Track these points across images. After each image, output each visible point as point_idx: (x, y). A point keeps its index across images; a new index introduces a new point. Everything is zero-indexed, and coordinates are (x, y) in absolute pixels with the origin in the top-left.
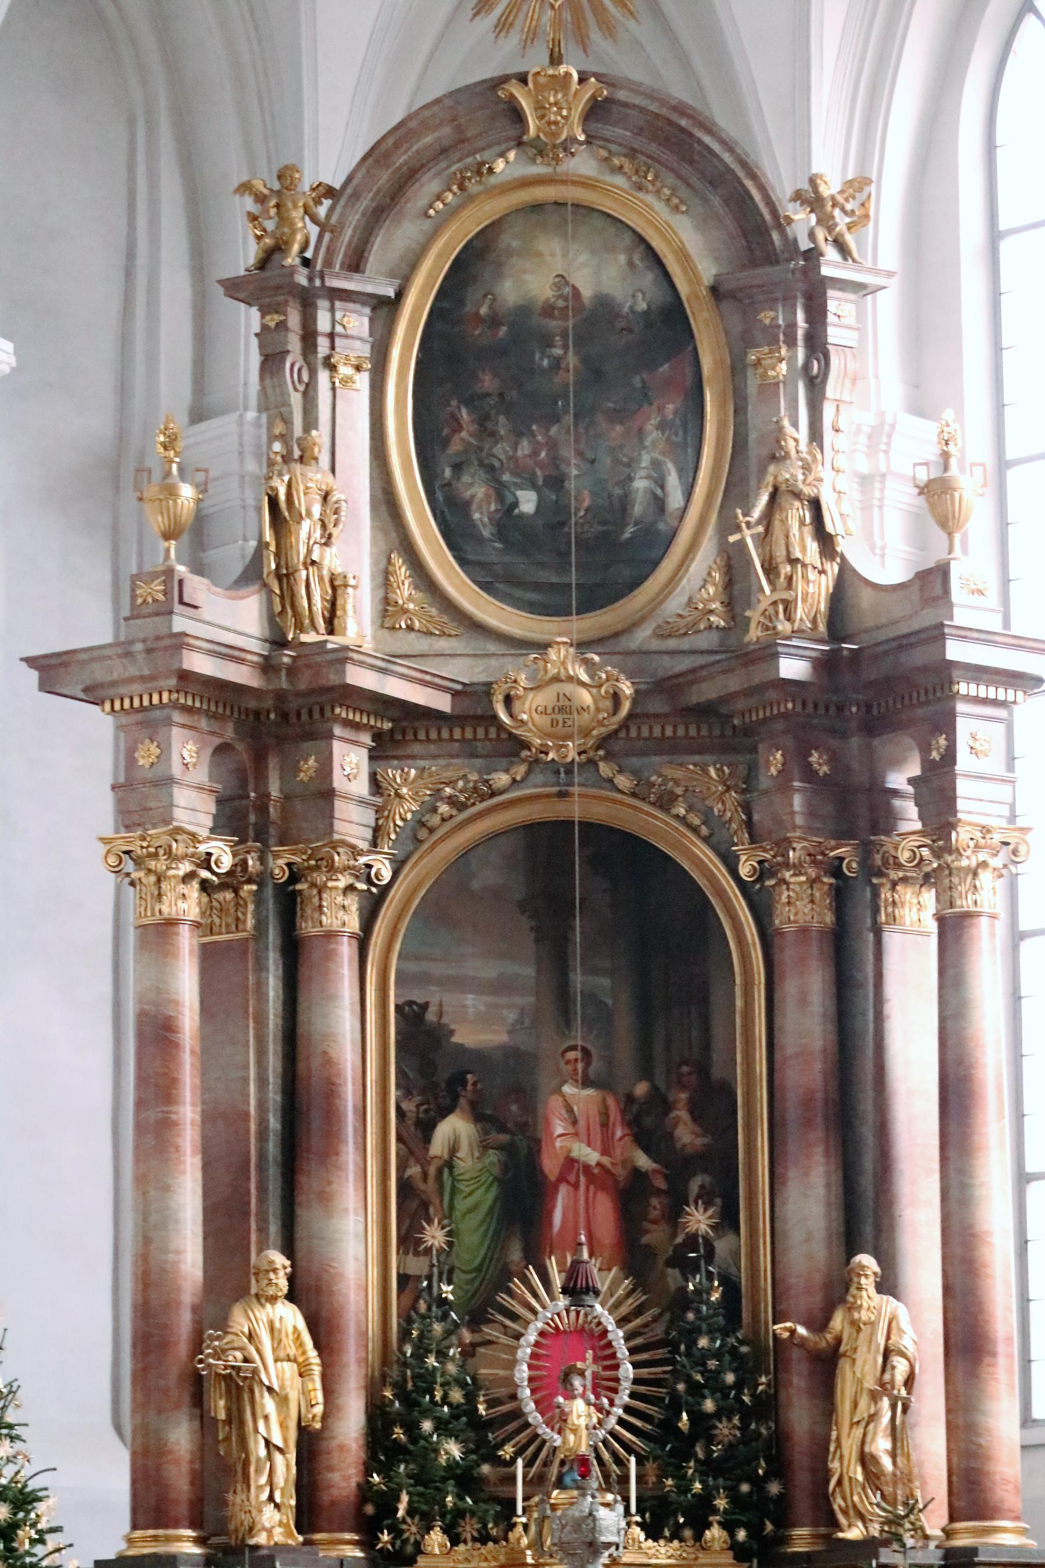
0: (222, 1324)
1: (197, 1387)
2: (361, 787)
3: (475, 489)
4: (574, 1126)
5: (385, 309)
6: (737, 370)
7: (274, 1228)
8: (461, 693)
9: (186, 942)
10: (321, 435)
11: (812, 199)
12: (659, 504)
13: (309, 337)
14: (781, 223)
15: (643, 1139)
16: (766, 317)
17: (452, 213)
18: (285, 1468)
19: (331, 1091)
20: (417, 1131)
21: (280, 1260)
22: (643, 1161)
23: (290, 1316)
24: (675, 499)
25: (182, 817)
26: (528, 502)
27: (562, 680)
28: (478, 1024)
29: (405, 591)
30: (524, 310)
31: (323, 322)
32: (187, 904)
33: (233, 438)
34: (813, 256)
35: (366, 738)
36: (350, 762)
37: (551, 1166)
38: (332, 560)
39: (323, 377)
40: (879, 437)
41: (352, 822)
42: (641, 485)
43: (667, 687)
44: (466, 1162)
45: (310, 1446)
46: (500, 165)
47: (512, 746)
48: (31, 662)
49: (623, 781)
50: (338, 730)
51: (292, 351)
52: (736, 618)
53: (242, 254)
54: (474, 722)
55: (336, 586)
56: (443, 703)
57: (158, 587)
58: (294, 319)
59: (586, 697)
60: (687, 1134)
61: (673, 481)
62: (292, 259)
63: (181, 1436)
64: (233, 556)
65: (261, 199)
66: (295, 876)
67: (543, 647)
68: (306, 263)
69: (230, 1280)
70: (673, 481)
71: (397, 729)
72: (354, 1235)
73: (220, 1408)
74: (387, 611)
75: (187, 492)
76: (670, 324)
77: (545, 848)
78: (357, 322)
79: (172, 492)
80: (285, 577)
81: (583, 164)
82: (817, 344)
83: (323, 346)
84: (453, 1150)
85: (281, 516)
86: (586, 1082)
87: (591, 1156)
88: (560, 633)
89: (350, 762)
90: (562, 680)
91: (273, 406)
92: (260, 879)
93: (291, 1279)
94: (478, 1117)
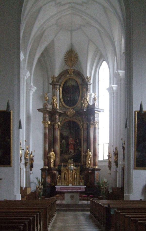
0: (49, 153)
1: (48, 157)
2: (58, 118)
3: (66, 98)
4: (71, 141)
5: (60, 86)
6: (82, 90)
7: (52, 147)
8: (64, 112)
9: (47, 128)
10: (56, 94)
11: (87, 78)
12: (77, 99)
13: (55, 88)
14: (85, 80)
15: (75, 142)
16: (84, 86)
17: (64, 79)
18: (53, 162)
19: (56, 139)
20: (61, 141)
21: (53, 149)
22: (75, 143)
23: (53, 153)
24: (78, 99)
25: (47, 120)
26: (69, 99)
27: (71, 111)
28: (65, 134)
29: (61, 105)
30: (69, 85)
31: (56, 86)
32: (47, 126)
33: (50, 94)
34: (87, 82)
35: (58, 115)
36: (57, 117)
37: (69, 143)
38: (56, 103)
39: (56, 90)
40: (91, 95)
41: (57, 120)
42: (76, 98)
43: (78, 111)
44: (64, 143)
45: (55, 161)
46: (67, 76)
47: (67, 115)
48: (38, 109)
49: (74, 118)
50: (56, 114)
51: (54, 88)
52: (82, 107)
53: (51, 81)
54: (65, 114)
55: (57, 104)
56: (63, 112)
57: (45, 104)
58: (54, 86)
59: (72, 112)
60: (78, 141)
61: (78, 98)
62: (54, 82)
63: (47, 160)
64: (50, 102)
65: (52, 78)
66: (54, 124)
67: (69, 109)
68: (55, 82)
69: (50, 151)
70: (78, 98)
71: (60, 114)
72: (57, 148)
73: (49, 158)
74: (60, 106)
75: (47, 98)
76: (78, 87)
77: (70, 122)
78: (58, 86)
79: (46, 98)
80: (53, 104)
81: (73, 75)
82: (87, 88)
83: (56, 88)
84: (64, 142)
85: (53, 100)
86: (72, 138)
87: (72, 143)
88: (71, 108)
89: (57, 117)
90: (71, 111)
91: (53, 92)
92: (52, 124)
93: (53, 150)
94: (65, 140)
